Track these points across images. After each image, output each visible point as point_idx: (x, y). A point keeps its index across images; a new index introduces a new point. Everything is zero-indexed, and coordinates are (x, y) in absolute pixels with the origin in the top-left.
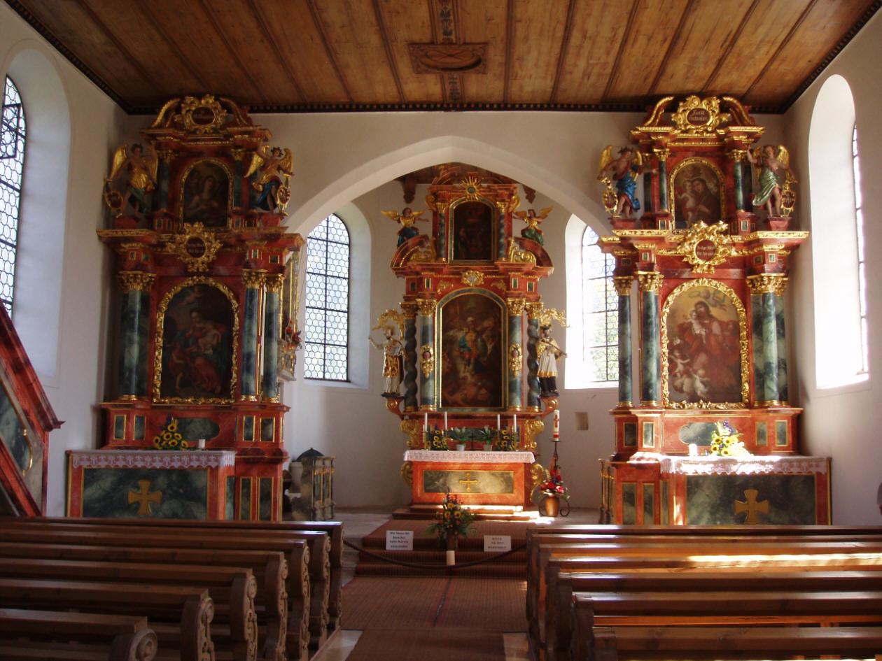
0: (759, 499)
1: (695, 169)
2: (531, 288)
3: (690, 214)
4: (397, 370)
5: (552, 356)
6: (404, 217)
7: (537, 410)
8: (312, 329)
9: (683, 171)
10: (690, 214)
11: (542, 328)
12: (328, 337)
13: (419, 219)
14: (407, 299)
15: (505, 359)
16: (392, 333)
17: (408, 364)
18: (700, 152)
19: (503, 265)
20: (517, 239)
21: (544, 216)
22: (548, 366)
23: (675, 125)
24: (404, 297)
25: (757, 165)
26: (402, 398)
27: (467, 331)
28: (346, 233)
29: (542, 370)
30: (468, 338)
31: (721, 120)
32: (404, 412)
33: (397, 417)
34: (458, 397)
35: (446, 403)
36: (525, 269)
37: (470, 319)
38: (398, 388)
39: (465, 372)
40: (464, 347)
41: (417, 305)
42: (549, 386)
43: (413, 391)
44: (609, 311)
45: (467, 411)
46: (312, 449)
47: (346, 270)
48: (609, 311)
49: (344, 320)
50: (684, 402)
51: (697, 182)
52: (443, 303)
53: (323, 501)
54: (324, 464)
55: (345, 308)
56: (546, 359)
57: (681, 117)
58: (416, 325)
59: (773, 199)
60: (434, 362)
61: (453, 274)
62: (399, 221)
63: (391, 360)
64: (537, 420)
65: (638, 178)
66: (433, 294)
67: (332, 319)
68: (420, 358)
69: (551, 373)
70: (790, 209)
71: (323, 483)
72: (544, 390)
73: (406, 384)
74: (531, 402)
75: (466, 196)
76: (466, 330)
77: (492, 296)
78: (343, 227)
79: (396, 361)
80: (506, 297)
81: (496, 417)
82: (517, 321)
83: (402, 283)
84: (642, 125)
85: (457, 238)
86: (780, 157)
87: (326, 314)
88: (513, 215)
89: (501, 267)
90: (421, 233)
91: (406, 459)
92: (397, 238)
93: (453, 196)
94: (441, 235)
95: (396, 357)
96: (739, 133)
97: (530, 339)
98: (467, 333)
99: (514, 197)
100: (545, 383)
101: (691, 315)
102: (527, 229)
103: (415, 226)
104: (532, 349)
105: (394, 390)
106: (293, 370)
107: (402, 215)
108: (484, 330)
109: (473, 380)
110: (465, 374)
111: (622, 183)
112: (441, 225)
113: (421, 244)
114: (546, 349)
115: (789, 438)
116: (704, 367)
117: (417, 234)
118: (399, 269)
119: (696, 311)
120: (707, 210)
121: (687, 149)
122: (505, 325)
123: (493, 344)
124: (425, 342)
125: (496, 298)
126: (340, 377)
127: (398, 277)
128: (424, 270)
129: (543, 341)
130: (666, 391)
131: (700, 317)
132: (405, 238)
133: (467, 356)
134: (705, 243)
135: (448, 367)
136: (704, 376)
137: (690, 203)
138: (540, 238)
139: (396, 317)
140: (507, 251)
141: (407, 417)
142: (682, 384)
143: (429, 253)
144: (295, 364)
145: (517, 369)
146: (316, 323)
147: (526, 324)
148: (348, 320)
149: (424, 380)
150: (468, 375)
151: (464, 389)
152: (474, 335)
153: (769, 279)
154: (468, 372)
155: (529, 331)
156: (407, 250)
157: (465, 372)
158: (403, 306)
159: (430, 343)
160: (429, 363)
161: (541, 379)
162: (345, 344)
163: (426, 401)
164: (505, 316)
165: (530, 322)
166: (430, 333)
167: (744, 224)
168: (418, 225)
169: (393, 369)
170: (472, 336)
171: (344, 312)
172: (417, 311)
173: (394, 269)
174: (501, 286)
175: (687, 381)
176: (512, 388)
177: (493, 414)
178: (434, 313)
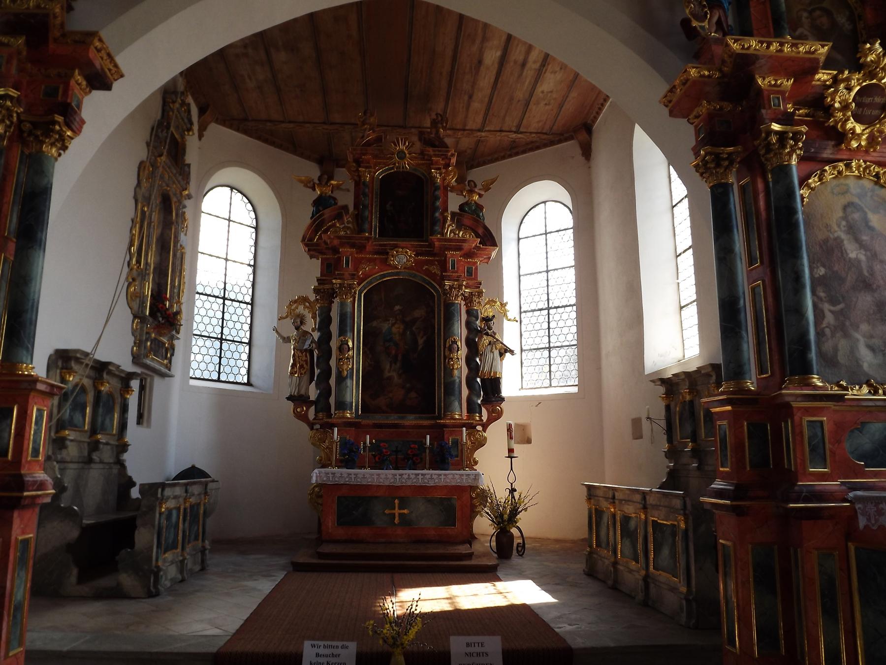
2: (470, 273)
5: (496, 353)
6: (320, 184)
7: (478, 418)
8: (206, 320)
12: (226, 331)
15: (439, 355)
20: (453, 214)
21: (487, 188)
24: (318, 280)
26: (312, 403)
28: (253, 215)
30: (394, 330)
32: (314, 419)
33: (305, 427)
35: (366, 408)
37: (397, 308)
38: (307, 389)
39: (391, 371)
41: (333, 289)
42: (492, 386)
43: (325, 393)
44: (551, 308)
45: (393, 419)
46: (193, 467)
48: (551, 308)
49: (247, 313)
50: (844, 383)
51: (818, 13)
53: (183, 549)
54: (186, 491)
56: (489, 356)
62: (314, 190)
63: (300, 354)
66: (353, 275)
67: (231, 310)
69: (495, 373)
71: (184, 520)
73: (317, 385)
75: (395, 164)
76: (392, 321)
77: (424, 280)
78: (249, 207)
83: (314, 267)
87: (224, 304)
91: (314, 480)
92: (311, 209)
93: (380, 163)
94: (365, 207)
95: (306, 350)
98: (393, 325)
101: (839, 226)
102: (466, 203)
105: (303, 392)
106: (170, 362)
107: (317, 182)
112: (365, 195)
113: (339, 217)
114: (490, 343)
117: (336, 204)
119: (845, 218)
123: (425, 338)
125: (429, 283)
126: (239, 379)
127: (311, 257)
128: (342, 245)
129: (487, 334)
132: (321, 208)
133: (394, 352)
139: (307, 304)
140: (443, 228)
141: (318, 426)
142: (836, 350)
143: (348, 228)
144: (172, 355)
146: (211, 313)
149: (341, 379)
150: (394, 374)
152: (402, 327)
155: (468, 324)
156: (322, 224)
157: (391, 371)
158: (316, 291)
159: (349, 334)
160: (347, 358)
163: (342, 405)
164: (439, 306)
165: (469, 312)
166: (349, 321)
168: (336, 194)
169: (301, 367)
174: (435, 270)
175: (843, 344)
178: (354, 298)
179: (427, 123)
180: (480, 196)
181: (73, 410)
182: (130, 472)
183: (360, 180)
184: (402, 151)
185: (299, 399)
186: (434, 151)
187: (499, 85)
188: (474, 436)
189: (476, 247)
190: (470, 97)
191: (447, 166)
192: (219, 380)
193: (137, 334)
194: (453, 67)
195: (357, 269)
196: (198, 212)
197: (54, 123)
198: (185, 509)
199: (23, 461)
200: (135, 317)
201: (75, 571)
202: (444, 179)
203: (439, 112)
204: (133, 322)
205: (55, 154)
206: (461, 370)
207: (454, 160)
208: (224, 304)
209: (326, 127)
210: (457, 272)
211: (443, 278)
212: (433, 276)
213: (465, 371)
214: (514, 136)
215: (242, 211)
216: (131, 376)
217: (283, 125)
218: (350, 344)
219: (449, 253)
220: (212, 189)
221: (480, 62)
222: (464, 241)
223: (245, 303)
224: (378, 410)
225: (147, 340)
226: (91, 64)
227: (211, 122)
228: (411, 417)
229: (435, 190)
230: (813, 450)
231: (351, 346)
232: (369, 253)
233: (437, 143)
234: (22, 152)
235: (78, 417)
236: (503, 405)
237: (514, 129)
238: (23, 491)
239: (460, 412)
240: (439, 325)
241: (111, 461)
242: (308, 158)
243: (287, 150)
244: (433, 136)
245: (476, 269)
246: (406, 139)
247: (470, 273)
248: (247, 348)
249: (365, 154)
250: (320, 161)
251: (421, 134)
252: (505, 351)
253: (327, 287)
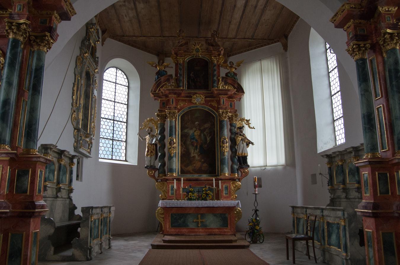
4: (154, 152)
5: (245, 144)
6: (159, 65)
7: (236, 176)
8: (106, 131)
12: (115, 136)
13: (167, 67)
14: (160, 111)
15: (218, 145)
16: (151, 131)
17: (160, 149)
19: (217, 90)
20: (223, 78)
21: (239, 65)
24: (158, 110)
26: (157, 169)
27: (195, 130)
28: (126, 80)
30: (196, 133)
32: (158, 177)
33: (153, 180)
34: (190, 168)
35: (183, 172)
36: (229, 93)
37: (197, 123)
40: (194, 139)
42: (243, 160)
43: (163, 165)
45: (196, 176)
47: (126, 100)
49: (125, 127)
52: (181, 114)
54: (102, 211)
55: (125, 120)
56: (242, 145)
58: (165, 126)
60: (176, 148)
61: (187, 97)
62: (156, 68)
63: (151, 146)
64: (237, 182)
66: (176, 107)
67: (117, 126)
68: (167, 145)
71: (101, 225)
72: (240, 164)
74: (232, 171)
76: (194, 129)
78: (125, 77)
79: (154, 147)
81: (212, 180)
82: (225, 123)
83: (157, 104)
85: (189, 77)
87: (114, 123)
88: (220, 66)
89: (216, 92)
90: (168, 74)
95: (153, 144)
97: (231, 134)
98: (195, 131)
99: (221, 56)
100: (241, 159)
102: (229, 72)
103: (165, 70)
105: (152, 164)
106: (90, 151)
108: (205, 129)
109: (199, 158)
110: (194, 155)
113: (168, 80)
114: (242, 140)
118: (155, 94)
122: (217, 127)
123: (210, 137)
124: (171, 135)
127: (155, 99)
128: (170, 93)
129: (240, 135)
132: (159, 76)
133: (195, 144)
135: (184, 151)
138: (236, 78)
140: (218, 84)
141: (160, 180)
143: (173, 85)
144: (91, 147)
145: (226, 151)
146: (108, 127)
147: (229, 127)
148: (127, 127)
149: (170, 158)
150: (196, 155)
151: (194, 163)
152: (199, 132)
154: (196, 153)
155: (231, 130)
156: (160, 83)
157: (194, 153)
158: (158, 115)
159: (174, 136)
160: (173, 148)
161: (239, 157)
162: (125, 140)
163: (171, 170)
164: (217, 121)
165: (231, 125)
166: (174, 130)
169: (151, 152)
170: (198, 133)
171: (125, 122)
172: (166, 118)
173: (153, 94)
174: (214, 104)
176: (222, 162)
177: (211, 178)
178: (176, 118)
179: (209, 35)
180: (236, 69)
181: (49, 173)
182: (74, 202)
183: (178, 62)
184: (198, 49)
185: (151, 168)
186: (213, 48)
187: (244, 17)
188: (235, 184)
189: (234, 93)
190: (230, 22)
191: (219, 55)
192: (112, 159)
193: (76, 137)
194: (222, 8)
195: (177, 105)
196: (101, 79)
197: (45, 36)
198: (101, 219)
199: (34, 195)
200: (75, 129)
201: (52, 249)
202: (218, 61)
203: (215, 30)
204: (74, 131)
205: (46, 51)
207: (222, 52)
208: (114, 123)
209: (160, 38)
210: (225, 105)
211: (218, 108)
212: (213, 107)
214: (250, 40)
215: (122, 79)
216: (74, 157)
217: (141, 38)
218: (175, 140)
220: (108, 69)
221: (235, 6)
222: (229, 90)
223: (124, 122)
224: (188, 172)
225: (81, 140)
226: (62, 7)
227: (107, 37)
229: (214, 66)
231: (175, 142)
232: (184, 97)
233: (214, 44)
234: (30, 50)
235: (51, 176)
237: (250, 37)
238: (35, 209)
240: (217, 131)
241: (66, 197)
242: (152, 53)
243: (142, 49)
244: (212, 41)
246: (199, 43)
247: (231, 106)
248: (125, 143)
249: (180, 50)
250: (158, 55)
251: (207, 40)
253: (163, 113)
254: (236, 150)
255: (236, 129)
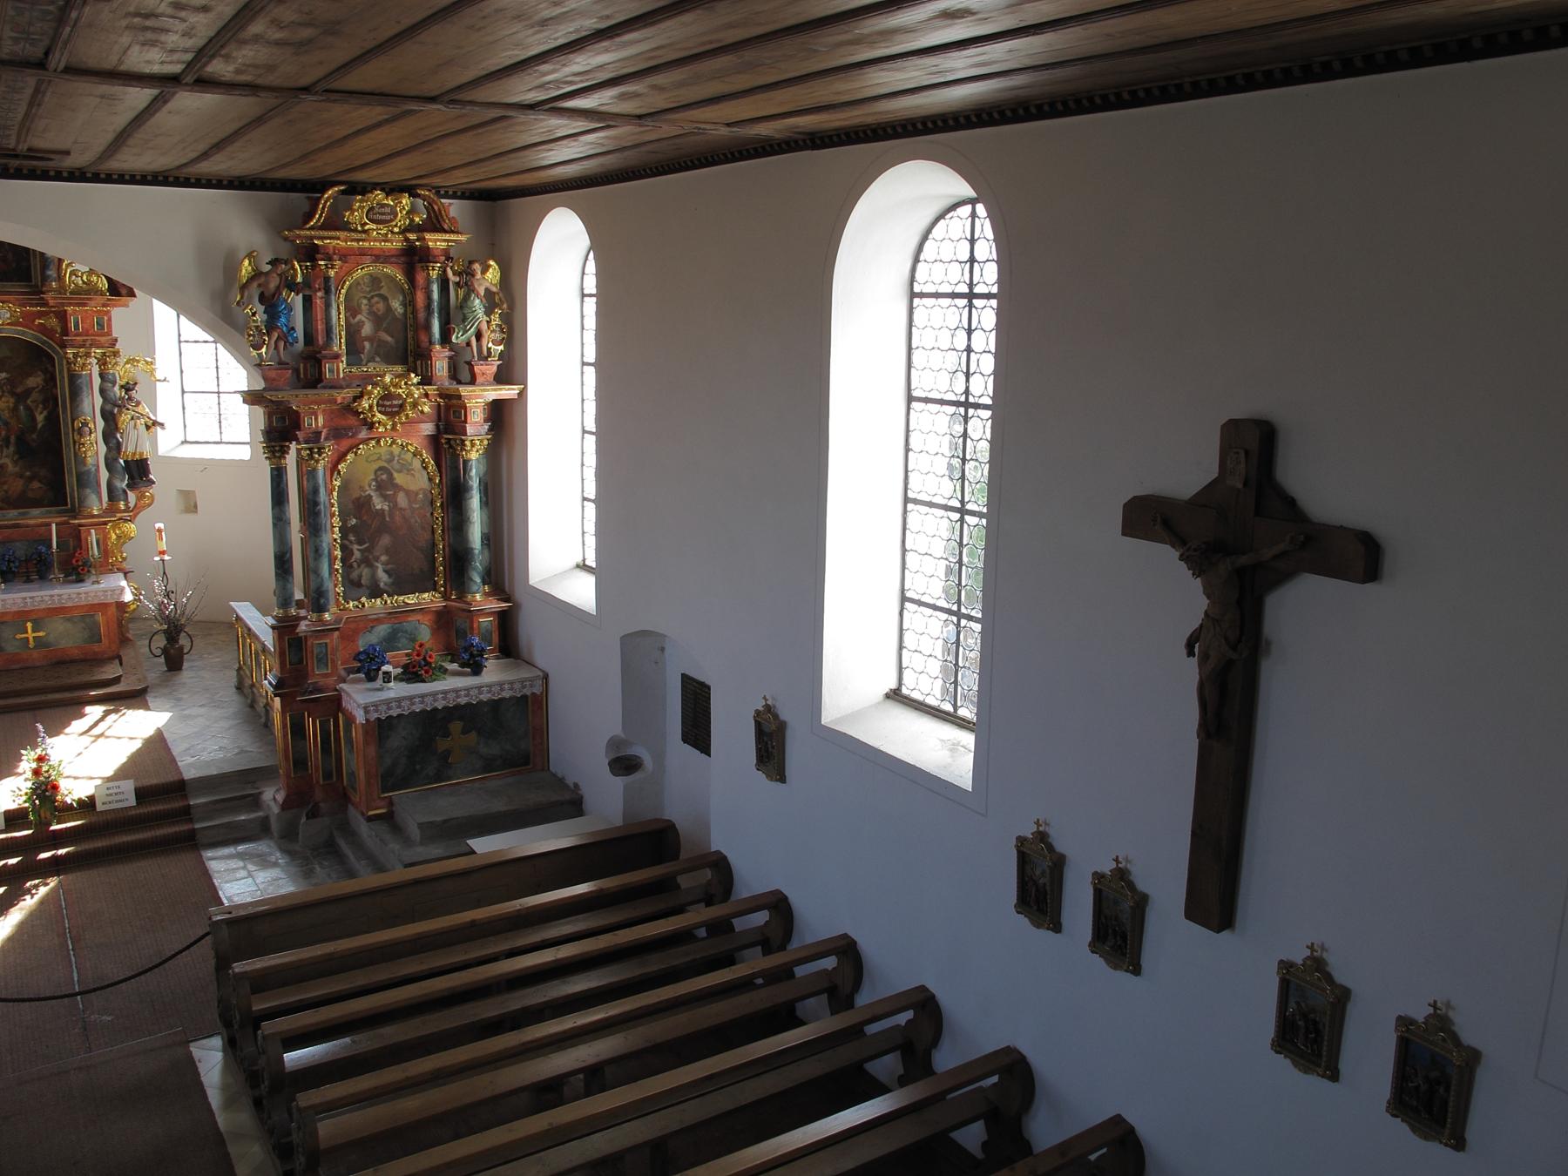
0: (465, 731)
1: (375, 281)
2: (100, 325)
3: (367, 344)
9: (357, 283)
10: (367, 344)
11: (122, 387)
18: (380, 257)
22: (134, 442)
23: (346, 227)
25: (457, 284)
29: (129, 449)
31: (412, 220)
42: (138, 471)
56: (133, 435)
57: (356, 216)
59: (479, 336)
65: (297, 301)
70: (501, 348)
72: (131, 478)
80: (64, 346)
84: (301, 229)
86: (489, 275)
89: (51, 302)
96: (436, 241)
104: (110, 418)
108: (28, 392)
111: (271, 304)
115: (495, 638)
116: (387, 551)
119: (375, 480)
120: (389, 339)
121: (362, 253)
125: (44, 343)
130: (340, 589)
131: (380, 487)
134: (387, 396)
136: (386, 563)
137: (367, 329)
142: (360, 576)
153: (473, 445)
155: (102, 391)
164: (61, 371)
165: (101, 375)
167: (440, 366)
175: (366, 572)
206: (95, 449)
213: (103, 449)
219: (69, 309)
228: (36, 512)
230: (319, 661)
236: (153, 490)
239: (96, 504)
240: (63, 395)
245: (110, 319)
252: (153, 425)
254: (119, 445)
255: (117, 388)
